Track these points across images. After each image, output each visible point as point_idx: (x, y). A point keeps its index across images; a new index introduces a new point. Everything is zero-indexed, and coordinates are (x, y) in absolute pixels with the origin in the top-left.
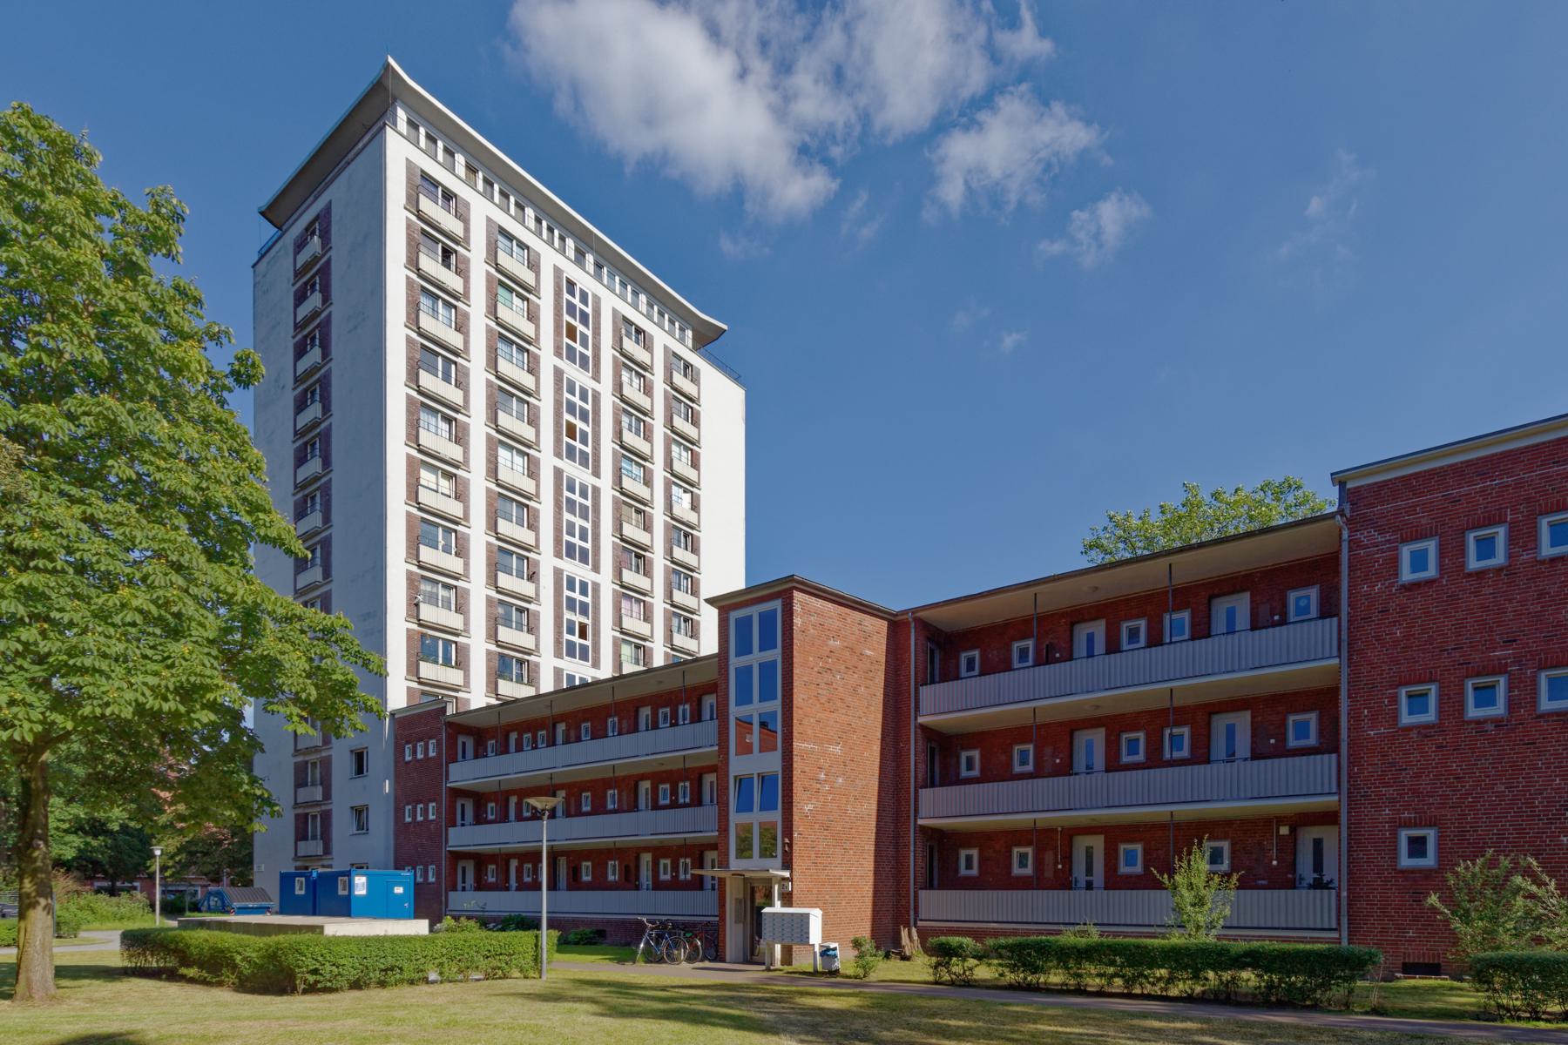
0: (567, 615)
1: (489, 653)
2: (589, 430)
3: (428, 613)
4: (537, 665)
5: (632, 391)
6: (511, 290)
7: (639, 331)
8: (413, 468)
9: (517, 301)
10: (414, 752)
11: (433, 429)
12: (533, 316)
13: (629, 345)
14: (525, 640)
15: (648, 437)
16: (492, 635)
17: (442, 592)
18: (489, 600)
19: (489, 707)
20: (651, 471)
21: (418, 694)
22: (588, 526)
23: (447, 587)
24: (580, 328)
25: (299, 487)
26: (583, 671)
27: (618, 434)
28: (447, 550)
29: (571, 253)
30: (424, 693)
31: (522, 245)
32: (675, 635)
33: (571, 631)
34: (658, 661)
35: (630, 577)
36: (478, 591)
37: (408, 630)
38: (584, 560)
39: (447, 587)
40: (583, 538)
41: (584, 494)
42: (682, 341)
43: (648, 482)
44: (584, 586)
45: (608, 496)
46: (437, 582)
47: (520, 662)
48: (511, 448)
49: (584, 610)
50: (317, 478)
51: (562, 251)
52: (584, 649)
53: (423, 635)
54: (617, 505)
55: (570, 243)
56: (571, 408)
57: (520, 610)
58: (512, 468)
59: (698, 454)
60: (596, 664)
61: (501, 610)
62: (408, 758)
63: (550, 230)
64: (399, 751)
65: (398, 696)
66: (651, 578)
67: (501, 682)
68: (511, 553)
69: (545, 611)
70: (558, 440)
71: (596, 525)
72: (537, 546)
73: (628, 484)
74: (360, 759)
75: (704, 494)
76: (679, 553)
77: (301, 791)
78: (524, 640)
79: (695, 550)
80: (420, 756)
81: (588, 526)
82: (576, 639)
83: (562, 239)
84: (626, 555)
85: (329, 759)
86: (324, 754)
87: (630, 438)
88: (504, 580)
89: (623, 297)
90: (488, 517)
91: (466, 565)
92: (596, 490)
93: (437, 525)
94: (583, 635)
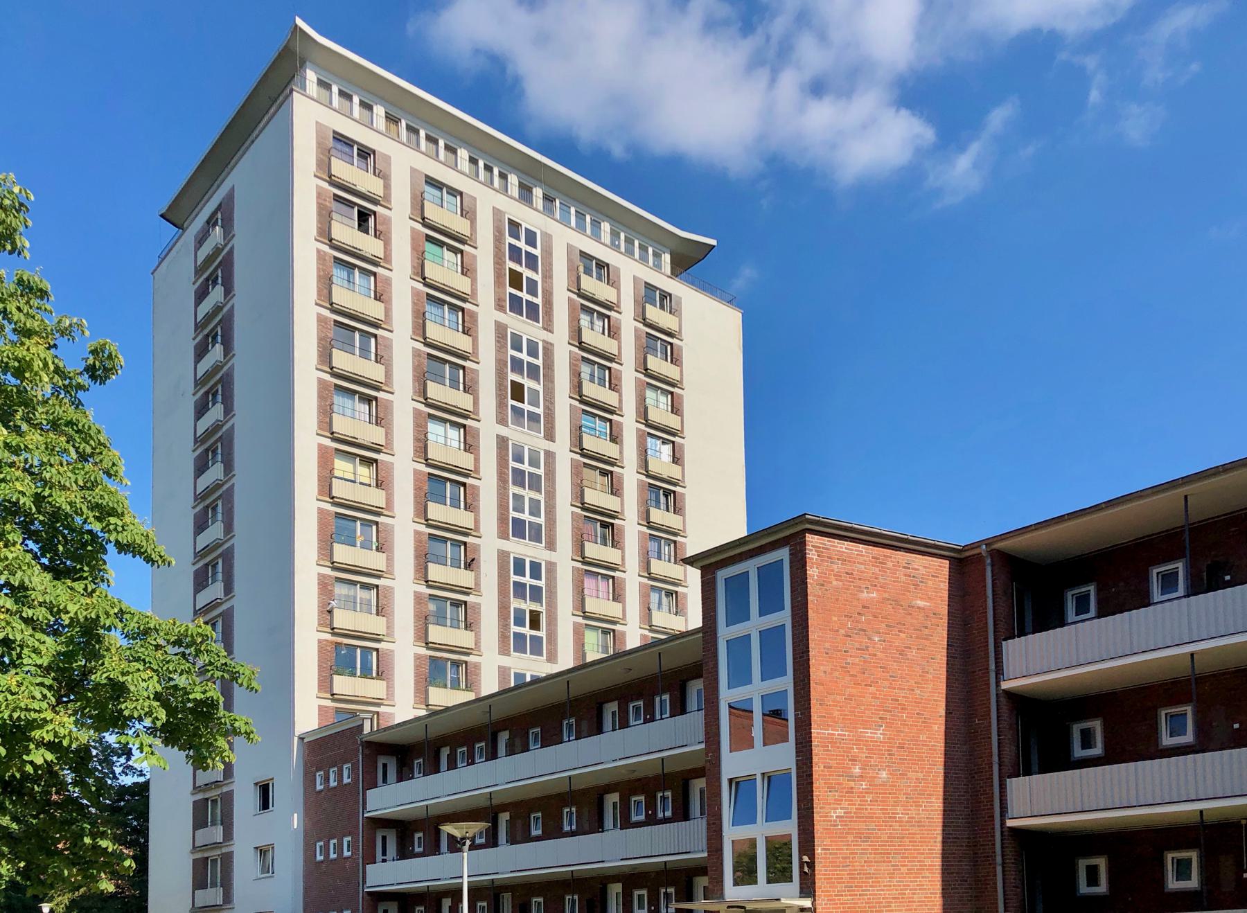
0: (515, 604)
1: (418, 658)
2: (540, 388)
3: (343, 619)
4: (477, 666)
5: (594, 336)
6: (441, 244)
7: (601, 265)
8: (325, 460)
9: (448, 255)
10: (327, 780)
11: (348, 412)
12: (467, 270)
13: (590, 284)
14: (462, 638)
15: (614, 387)
16: (422, 636)
17: (361, 594)
18: (418, 597)
19: (418, 719)
20: (620, 424)
21: (332, 713)
22: (541, 497)
23: (365, 586)
24: (527, 273)
25: (200, 498)
26: (535, 667)
27: (578, 387)
28: (366, 546)
29: (514, 190)
30: (338, 711)
31: (454, 192)
32: (655, 613)
33: (519, 622)
34: (633, 642)
35: (594, 551)
36: (404, 588)
37: (320, 641)
38: (536, 537)
39: (365, 586)
40: (535, 511)
41: (534, 462)
42: (658, 267)
43: (615, 439)
44: (536, 568)
45: (565, 458)
46: (354, 583)
47: (456, 664)
48: (445, 421)
49: (536, 594)
50: (218, 486)
51: (505, 190)
52: (536, 641)
53: (338, 645)
54: (576, 470)
55: (513, 179)
56: (517, 365)
57: (456, 604)
58: (445, 443)
59: (681, 397)
60: (552, 658)
61: (432, 607)
62: (319, 787)
63: (488, 168)
64: (309, 780)
65: (308, 715)
66: (622, 549)
67: (433, 691)
68: (445, 540)
69: (487, 603)
70: (501, 405)
71: (551, 495)
72: (477, 528)
73: (589, 443)
74: (265, 791)
75: (690, 444)
76: (658, 516)
77: (199, 832)
78: (462, 638)
79: (678, 510)
80: (333, 784)
81: (541, 497)
82: (526, 630)
83: (503, 176)
84: (590, 525)
85: (231, 793)
86: (225, 789)
87: (590, 390)
88: (436, 572)
89: (581, 228)
90: (417, 502)
91: (390, 561)
92: (550, 455)
93: (355, 519)
94: (535, 624)
